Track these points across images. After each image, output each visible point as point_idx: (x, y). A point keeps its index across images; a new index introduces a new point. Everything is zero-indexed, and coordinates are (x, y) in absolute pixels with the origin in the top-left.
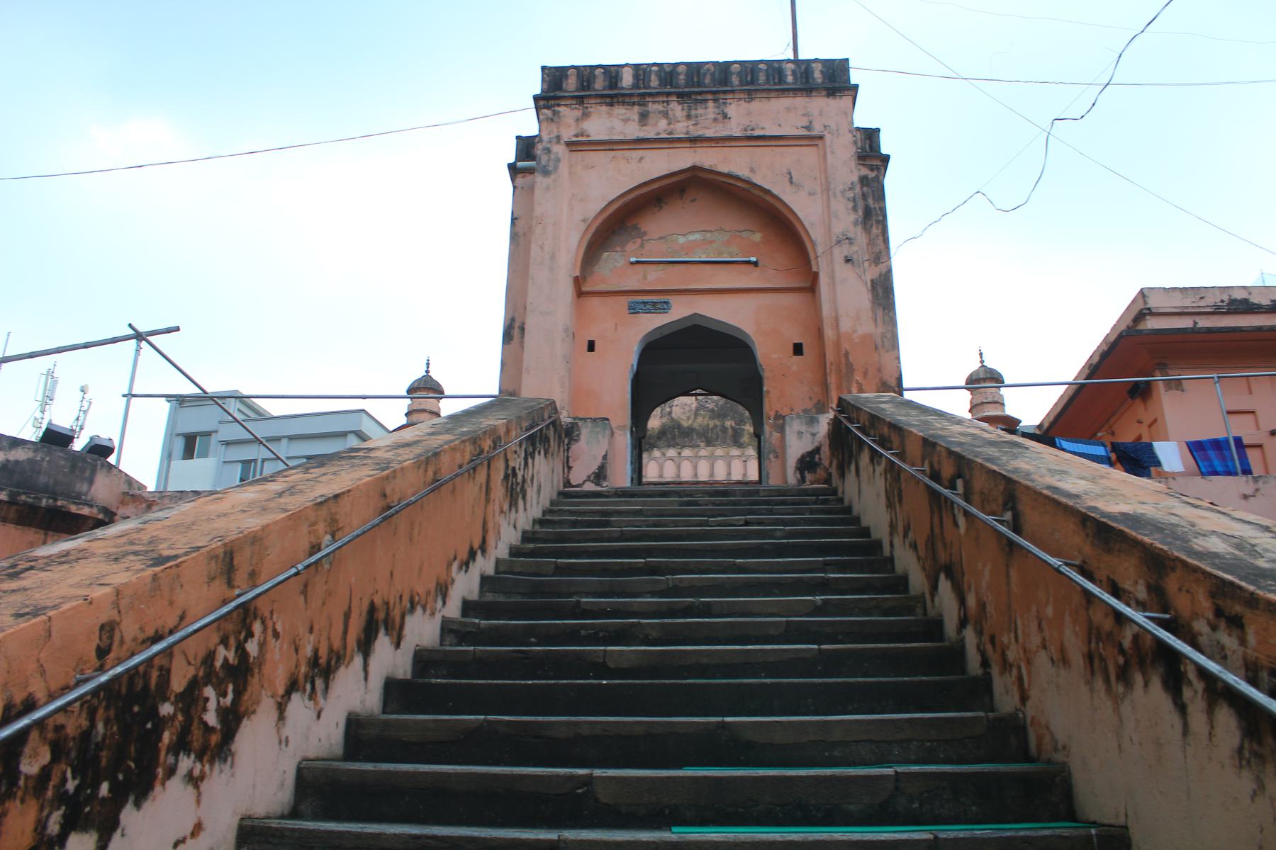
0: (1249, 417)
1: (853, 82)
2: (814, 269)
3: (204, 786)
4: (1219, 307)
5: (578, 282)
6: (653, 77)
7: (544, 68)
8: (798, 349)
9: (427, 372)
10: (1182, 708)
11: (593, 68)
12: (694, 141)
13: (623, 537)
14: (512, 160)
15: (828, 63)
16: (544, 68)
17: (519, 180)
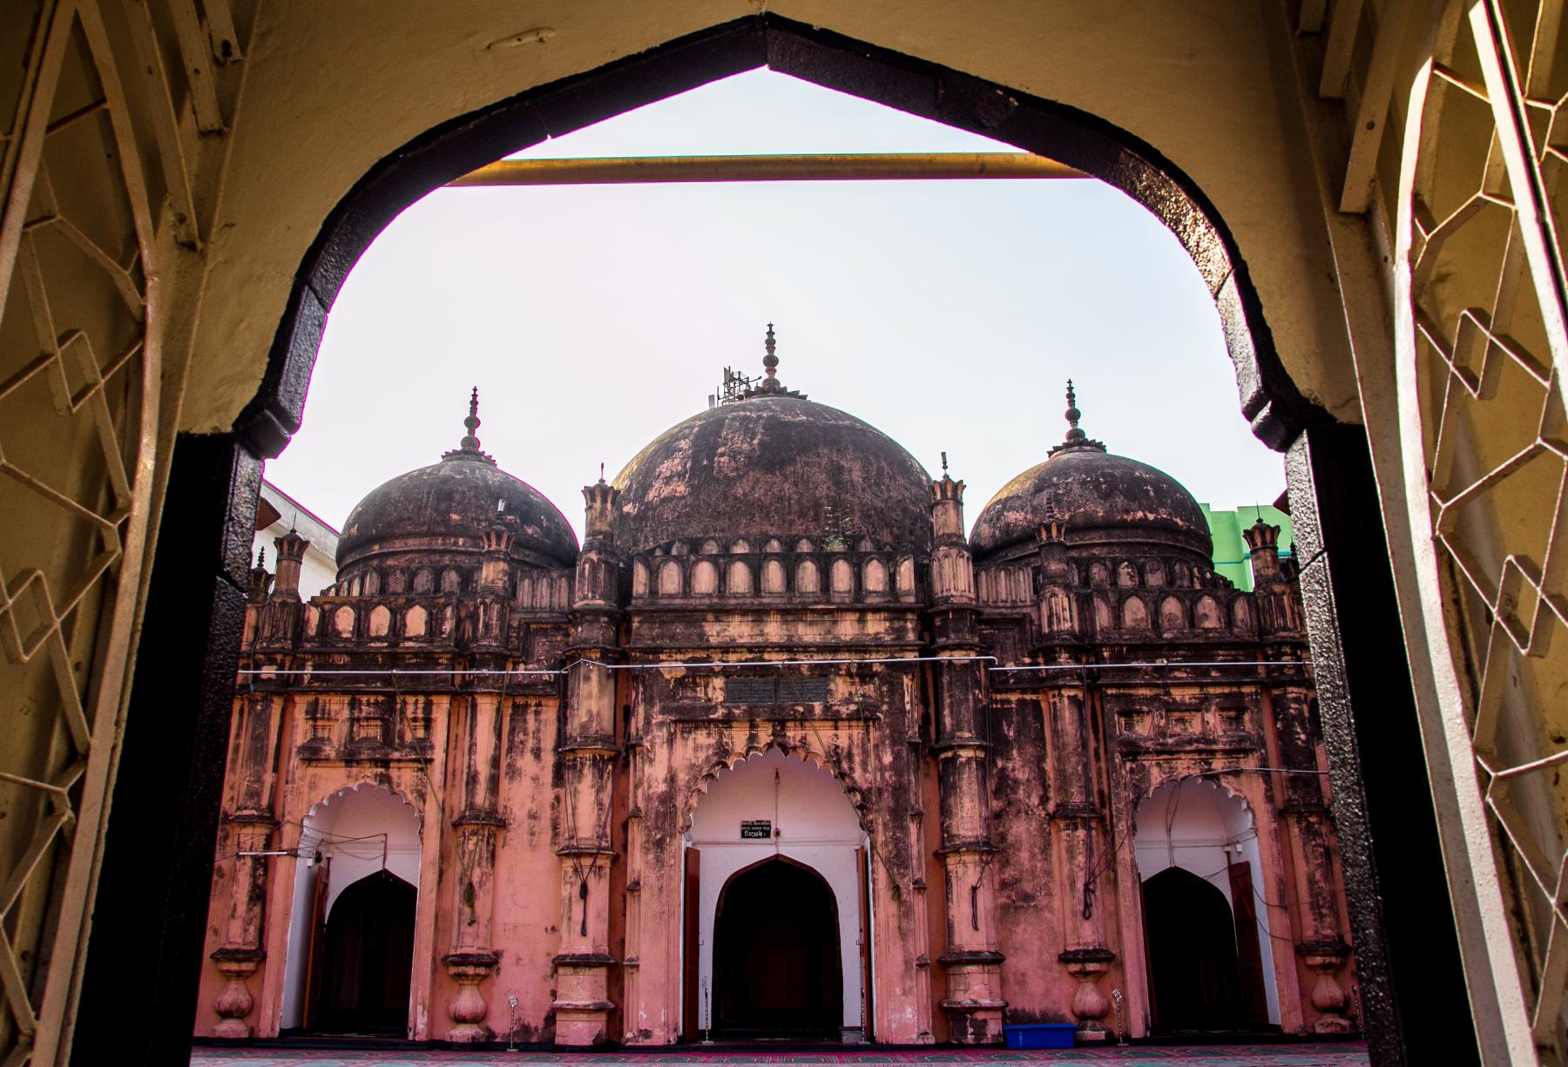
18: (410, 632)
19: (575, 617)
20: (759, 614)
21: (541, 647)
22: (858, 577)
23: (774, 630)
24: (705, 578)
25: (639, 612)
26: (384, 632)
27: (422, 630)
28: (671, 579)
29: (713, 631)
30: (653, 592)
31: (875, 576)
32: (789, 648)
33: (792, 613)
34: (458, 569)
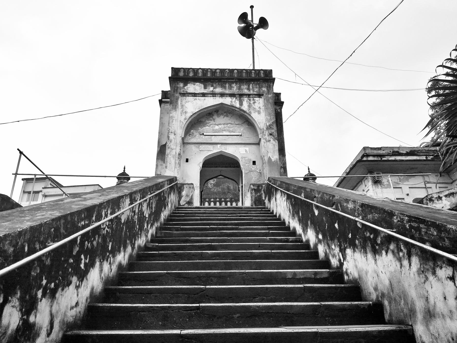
0: (400, 189)
1: (274, 76)
3: (79, 290)
4: (389, 153)
5: (183, 139)
6: (209, 73)
7: (172, 68)
8: (254, 163)
9: (124, 171)
10: (400, 260)
11: (189, 69)
12: (222, 95)
13: (201, 220)
14: (160, 99)
15: (265, 71)
16: (172, 68)
17: (163, 105)
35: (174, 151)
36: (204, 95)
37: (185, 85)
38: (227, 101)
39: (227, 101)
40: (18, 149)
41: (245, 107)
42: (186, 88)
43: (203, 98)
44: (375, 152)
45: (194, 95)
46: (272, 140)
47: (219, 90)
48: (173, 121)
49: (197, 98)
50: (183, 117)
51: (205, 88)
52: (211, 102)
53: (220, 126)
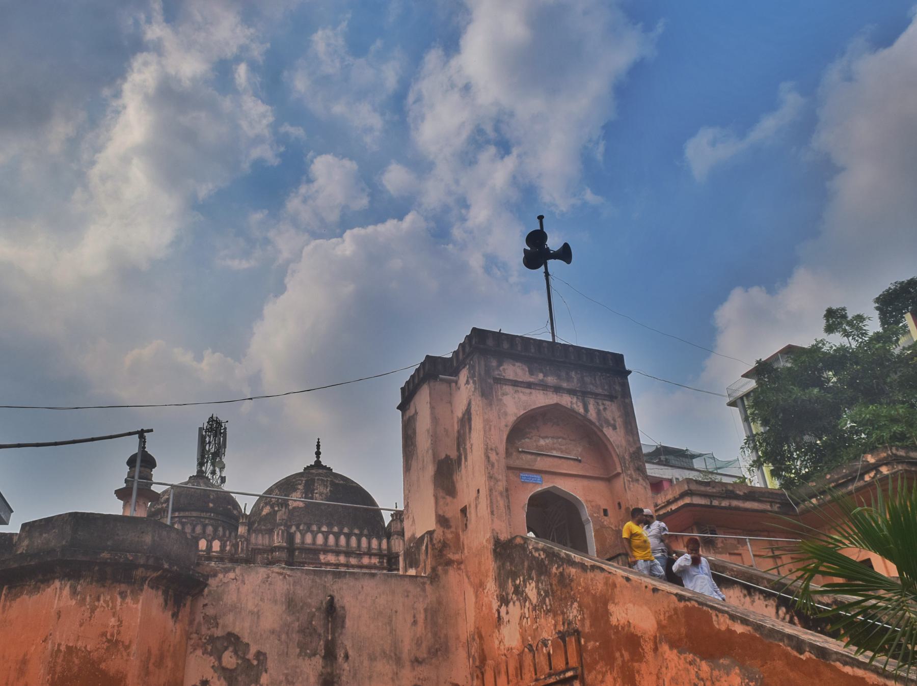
2: (619, 470)
12: (557, 390)
18: (214, 550)
19: (273, 549)
20: (337, 553)
21: (259, 557)
22: (369, 543)
23: (342, 559)
24: (320, 539)
25: (298, 549)
26: (204, 548)
27: (218, 549)
28: (309, 538)
29: (322, 557)
30: (303, 543)
31: (375, 543)
32: (347, 565)
33: (348, 553)
34: (212, 525)
35: (500, 483)
36: (529, 385)
37: (500, 364)
38: (566, 400)
39: (566, 400)
40: (151, 431)
41: (592, 415)
42: (501, 368)
43: (528, 391)
44: (702, 488)
45: (515, 383)
46: (640, 478)
47: (551, 380)
48: (490, 429)
49: (519, 389)
50: (503, 424)
51: (531, 373)
52: (541, 399)
53: (547, 441)
